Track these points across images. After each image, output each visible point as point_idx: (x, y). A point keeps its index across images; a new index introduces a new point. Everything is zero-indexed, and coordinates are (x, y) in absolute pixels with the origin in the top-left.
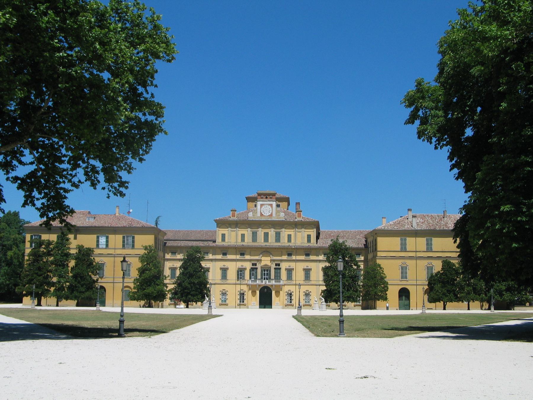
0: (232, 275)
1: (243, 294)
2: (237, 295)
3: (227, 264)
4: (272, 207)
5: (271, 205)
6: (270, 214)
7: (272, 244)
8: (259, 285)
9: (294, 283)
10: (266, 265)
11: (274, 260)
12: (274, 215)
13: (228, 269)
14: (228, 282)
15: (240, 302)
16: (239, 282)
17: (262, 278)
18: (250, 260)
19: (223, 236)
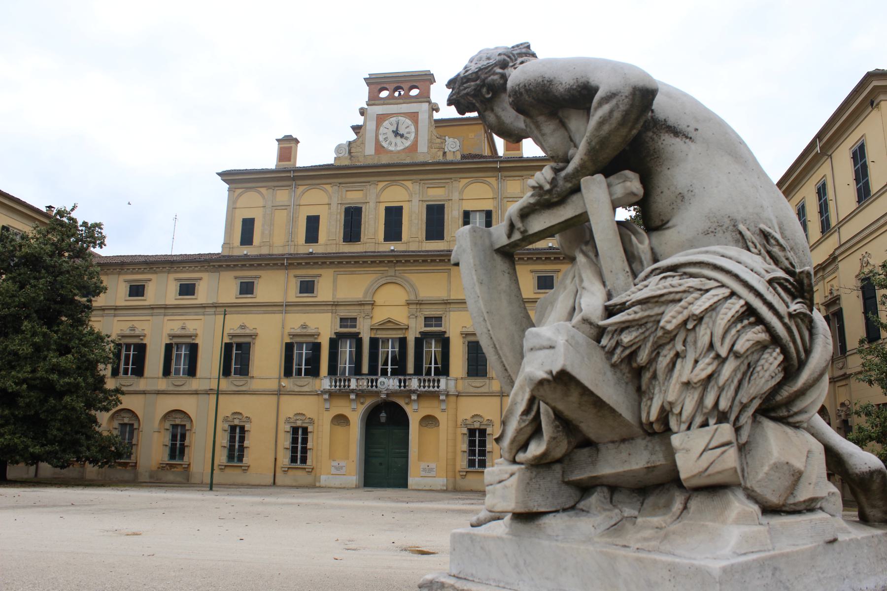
0: (266, 360)
1: (305, 431)
2: (281, 435)
3: (253, 322)
4: (416, 122)
5: (414, 117)
6: (407, 143)
7: (413, 247)
8: (360, 394)
9: (496, 386)
10: (389, 321)
11: (420, 303)
12: (423, 147)
13: (254, 336)
14: (255, 385)
15: (294, 460)
16: (285, 382)
17: (373, 370)
18: (336, 304)
19: (248, 225)
